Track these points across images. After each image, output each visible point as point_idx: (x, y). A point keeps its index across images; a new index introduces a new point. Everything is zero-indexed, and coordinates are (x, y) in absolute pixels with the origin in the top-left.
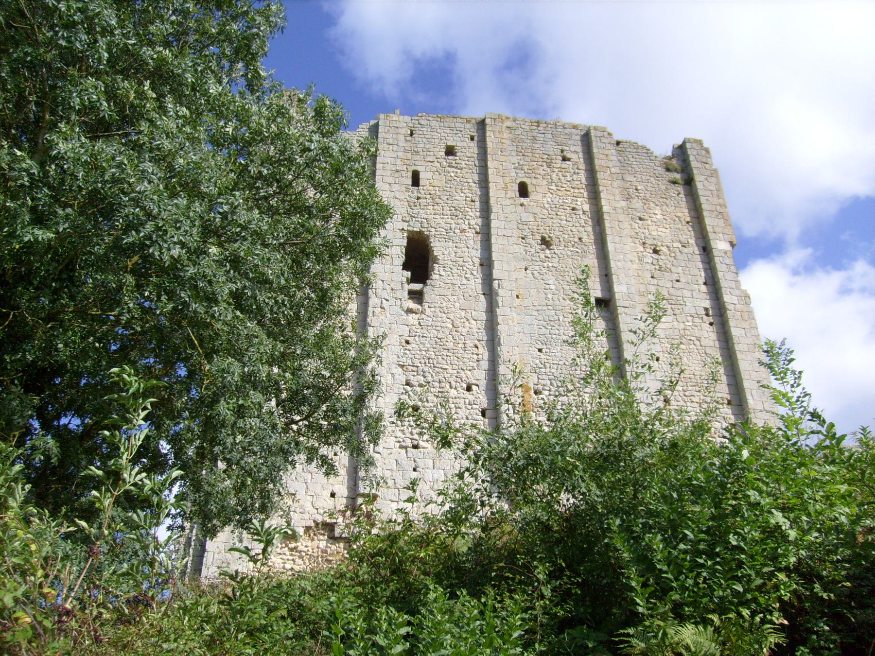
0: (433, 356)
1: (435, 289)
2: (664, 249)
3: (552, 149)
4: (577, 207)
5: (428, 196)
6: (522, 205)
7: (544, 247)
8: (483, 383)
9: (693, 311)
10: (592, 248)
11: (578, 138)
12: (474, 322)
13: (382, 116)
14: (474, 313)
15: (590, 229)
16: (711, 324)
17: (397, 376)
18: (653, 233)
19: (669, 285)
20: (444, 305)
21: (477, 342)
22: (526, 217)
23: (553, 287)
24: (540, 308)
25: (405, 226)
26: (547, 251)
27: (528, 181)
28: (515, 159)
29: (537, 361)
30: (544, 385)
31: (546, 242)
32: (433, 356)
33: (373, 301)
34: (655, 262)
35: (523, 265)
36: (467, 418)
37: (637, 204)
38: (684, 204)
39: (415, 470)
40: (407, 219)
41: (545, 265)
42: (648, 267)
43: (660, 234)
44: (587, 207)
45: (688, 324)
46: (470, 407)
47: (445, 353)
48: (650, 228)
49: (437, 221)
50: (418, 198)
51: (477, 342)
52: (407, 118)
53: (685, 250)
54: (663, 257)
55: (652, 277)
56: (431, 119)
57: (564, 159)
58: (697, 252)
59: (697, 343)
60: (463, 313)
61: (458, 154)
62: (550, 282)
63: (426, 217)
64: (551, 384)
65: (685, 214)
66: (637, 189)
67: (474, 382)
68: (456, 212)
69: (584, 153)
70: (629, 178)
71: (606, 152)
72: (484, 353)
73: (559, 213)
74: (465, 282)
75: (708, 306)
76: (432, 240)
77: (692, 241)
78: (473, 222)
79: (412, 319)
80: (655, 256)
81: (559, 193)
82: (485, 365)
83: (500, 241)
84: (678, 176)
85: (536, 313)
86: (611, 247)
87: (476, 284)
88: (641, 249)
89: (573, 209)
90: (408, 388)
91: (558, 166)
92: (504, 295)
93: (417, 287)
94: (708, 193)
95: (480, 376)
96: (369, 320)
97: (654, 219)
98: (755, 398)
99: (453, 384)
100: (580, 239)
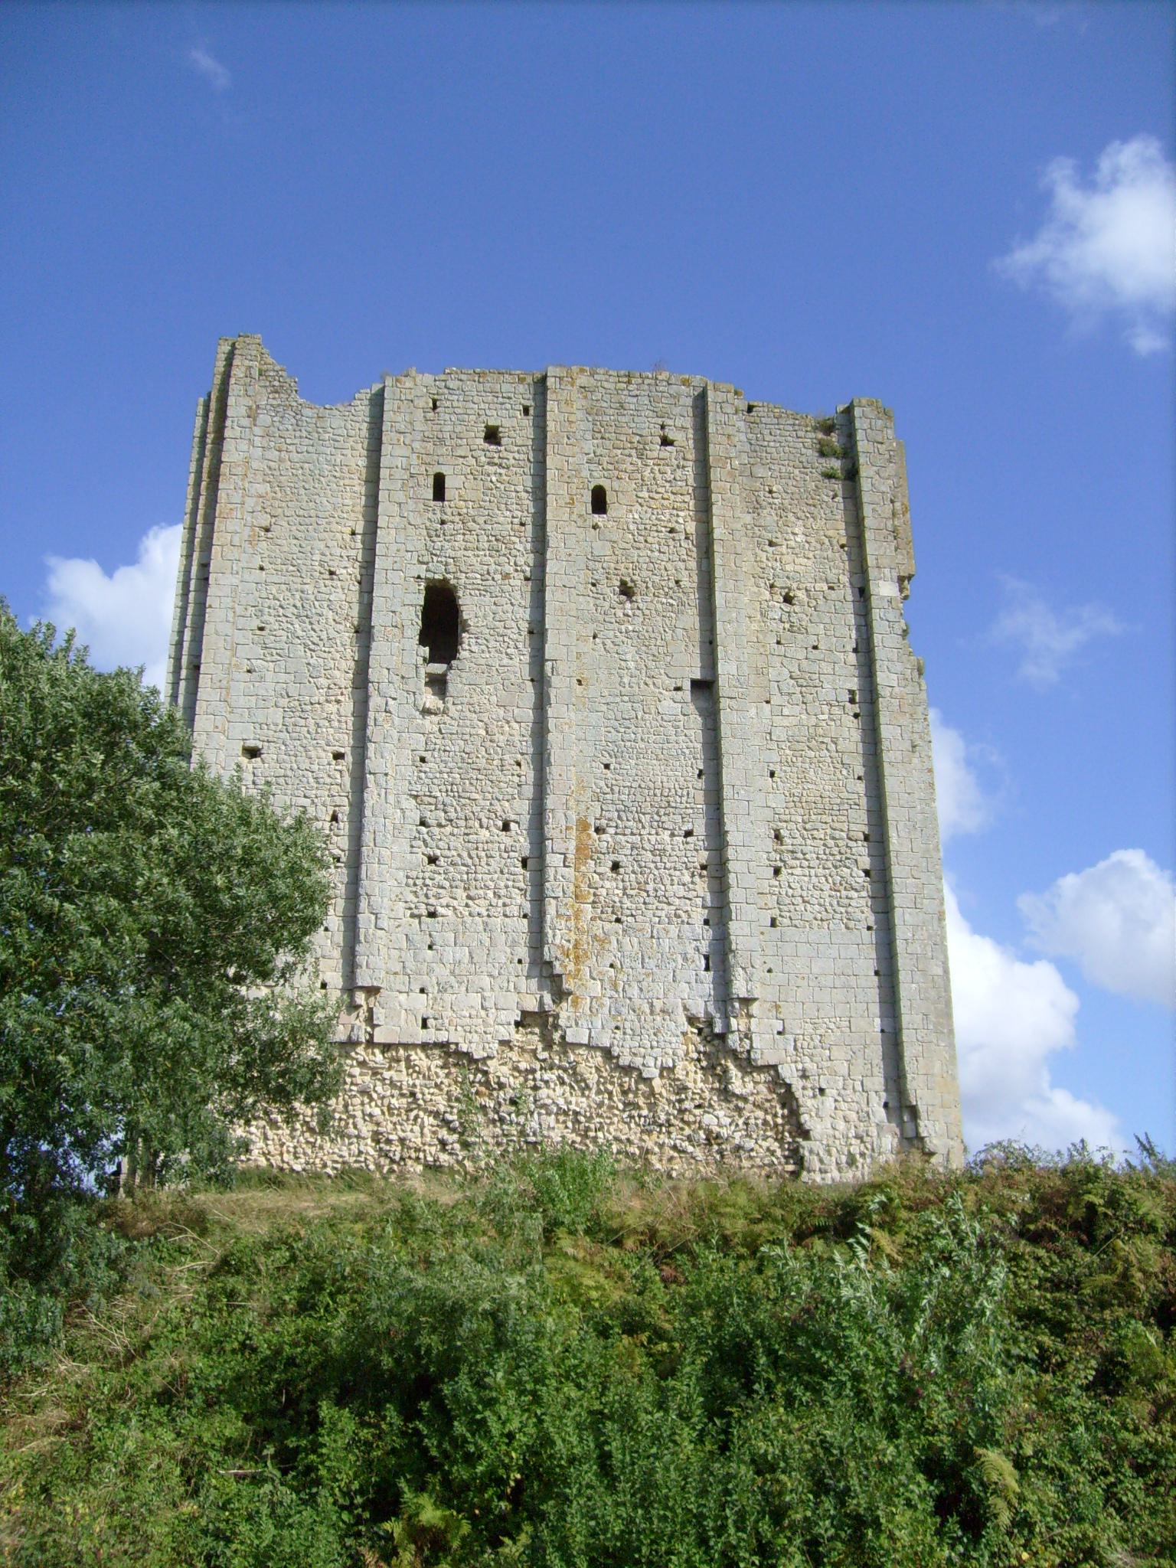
0: (458, 781)
1: (464, 674)
2: (801, 595)
3: (649, 427)
4: (677, 527)
5: (457, 519)
6: (595, 527)
7: (624, 598)
8: (525, 819)
9: (831, 697)
10: (694, 598)
11: (689, 401)
12: (516, 726)
13: (389, 382)
14: (516, 711)
15: (693, 565)
16: (856, 716)
17: (408, 813)
18: (788, 568)
19: (801, 655)
20: (475, 699)
21: (519, 757)
22: (602, 548)
23: (631, 665)
24: (612, 699)
25: (421, 571)
26: (628, 605)
27: (606, 484)
28: (589, 446)
29: (602, 784)
30: (610, 820)
31: (626, 591)
32: (458, 781)
33: (375, 701)
34: (785, 618)
35: (591, 628)
36: (502, 872)
37: (769, 517)
38: (839, 515)
39: (430, 947)
40: (425, 559)
41: (623, 628)
42: (774, 625)
43: (797, 568)
44: (691, 527)
45: (821, 717)
46: (506, 855)
47: (474, 774)
48: (784, 558)
49: (469, 561)
50: (443, 523)
51: (519, 757)
52: (428, 379)
53: (833, 595)
54: (797, 608)
55: (778, 643)
56: (463, 377)
57: (666, 442)
58: (850, 598)
59: (832, 747)
60: (501, 712)
61: (504, 441)
62: (629, 657)
63: (453, 554)
64: (619, 817)
65: (839, 532)
66: (770, 492)
67: (513, 817)
68: (498, 544)
69: (695, 430)
70: (760, 471)
71: (730, 430)
72: (528, 773)
73: (650, 539)
74: (506, 661)
75: (855, 688)
76: (460, 594)
77: (845, 579)
78: (521, 561)
79: (430, 723)
80: (786, 607)
81: (653, 504)
82: (529, 791)
83: (558, 595)
84: (836, 464)
85: (604, 708)
86: (719, 599)
87: (520, 663)
88: (767, 595)
89: (672, 531)
90: (424, 829)
91: (655, 454)
92: (559, 686)
93: (438, 668)
94: (877, 498)
95: (521, 809)
96: (369, 732)
97: (792, 543)
98: (902, 834)
99: (485, 820)
100: (677, 582)
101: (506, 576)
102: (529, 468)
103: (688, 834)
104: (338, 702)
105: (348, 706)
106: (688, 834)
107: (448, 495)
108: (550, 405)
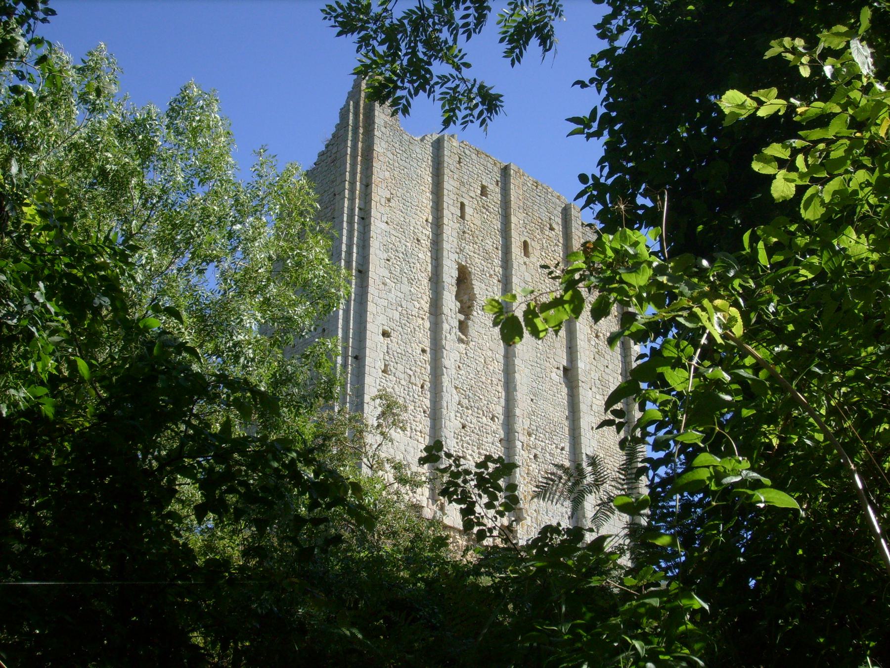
3: (545, 216)
8: (502, 417)
11: (560, 209)
27: (529, 241)
47: (481, 384)
95: (499, 410)
101: (491, 276)
103: (562, 449)
104: (423, 319)
105: (427, 325)
106: (562, 449)
107: (467, 217)
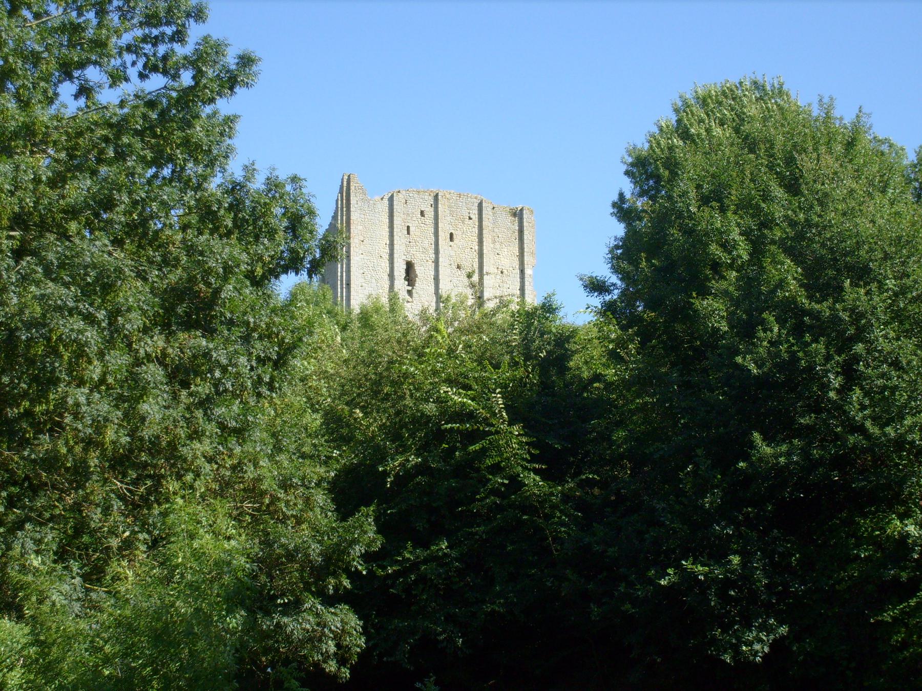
22: (453, 253)
35: (450, 279)
37: (498, 246)
38: (517, 246)
44: (477, 248)
57: (470, 218)
70: (496, 230)
93: (410, 288)
102: (432, 225)
108: (440, 206)
